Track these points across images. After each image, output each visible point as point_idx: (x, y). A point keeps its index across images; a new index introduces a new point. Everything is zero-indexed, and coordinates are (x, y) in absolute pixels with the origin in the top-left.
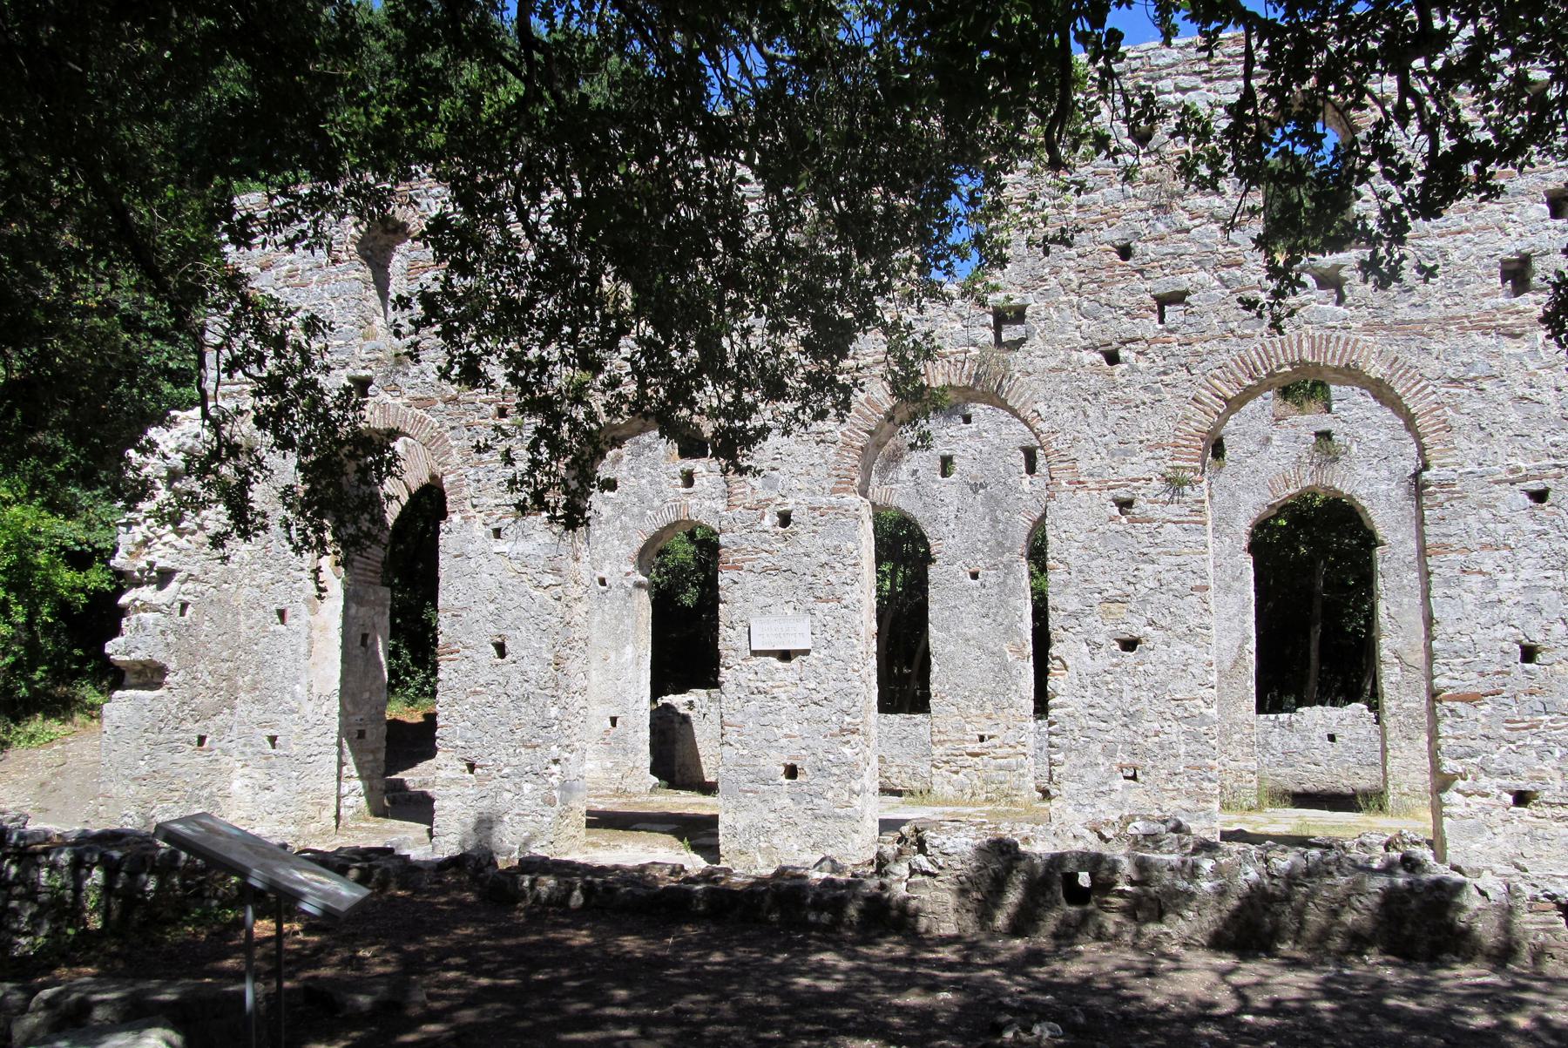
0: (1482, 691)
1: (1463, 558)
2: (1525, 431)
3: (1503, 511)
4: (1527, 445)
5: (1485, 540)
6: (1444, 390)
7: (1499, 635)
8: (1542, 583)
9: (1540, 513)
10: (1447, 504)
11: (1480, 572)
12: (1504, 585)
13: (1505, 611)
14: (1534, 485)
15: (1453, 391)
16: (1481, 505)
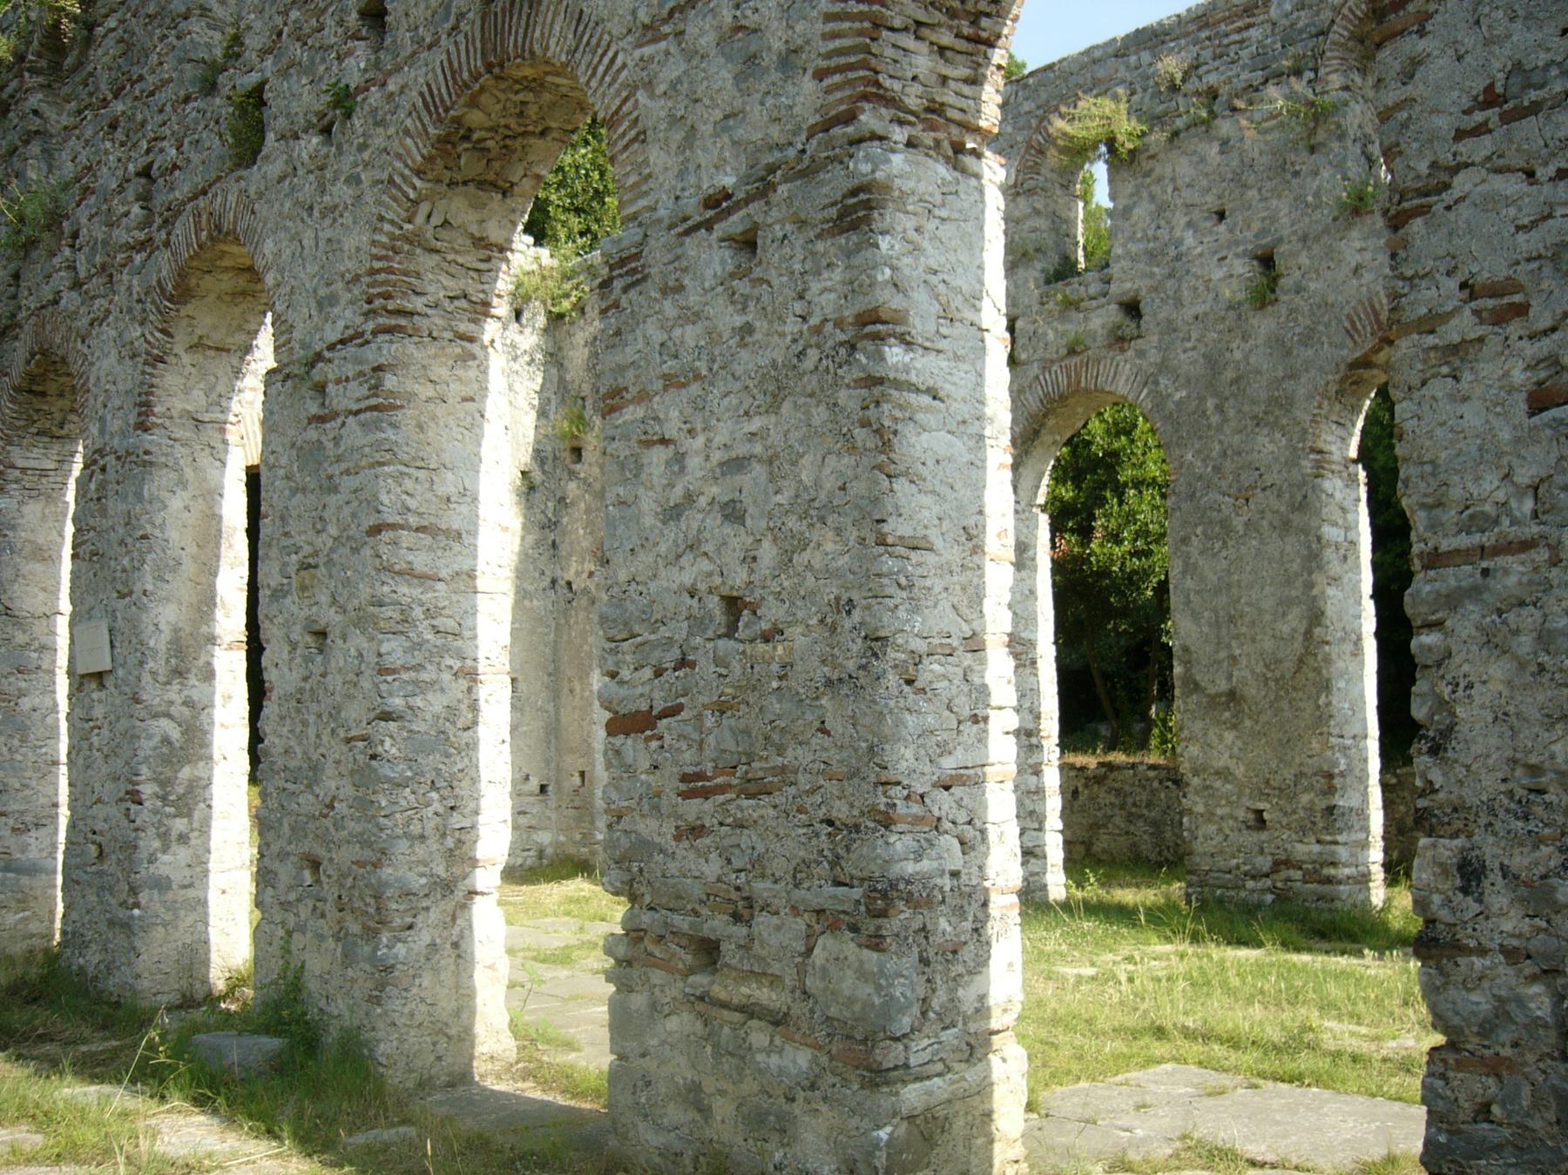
0: (659, 706)
1: (640, 412)
2: (738, 103)
3: (693, 299)
4: (740, 133)
5: (670, 365)
6: (637, 53)
7: (687, 578)
8: (741, 450)
9: (742, 287)
10: (624, 303)
11: (664, 441)
12: (693, 462)
13: (692, 521)
14: (735, 224)
15: (647, 51)
16: (665, 291)
